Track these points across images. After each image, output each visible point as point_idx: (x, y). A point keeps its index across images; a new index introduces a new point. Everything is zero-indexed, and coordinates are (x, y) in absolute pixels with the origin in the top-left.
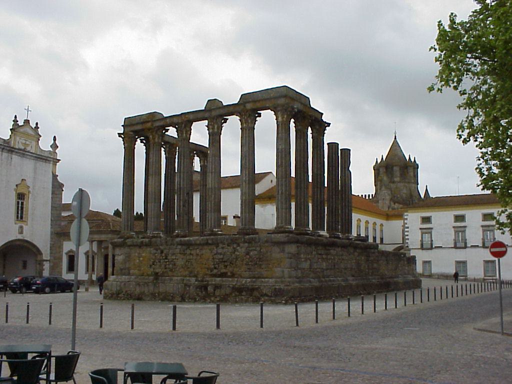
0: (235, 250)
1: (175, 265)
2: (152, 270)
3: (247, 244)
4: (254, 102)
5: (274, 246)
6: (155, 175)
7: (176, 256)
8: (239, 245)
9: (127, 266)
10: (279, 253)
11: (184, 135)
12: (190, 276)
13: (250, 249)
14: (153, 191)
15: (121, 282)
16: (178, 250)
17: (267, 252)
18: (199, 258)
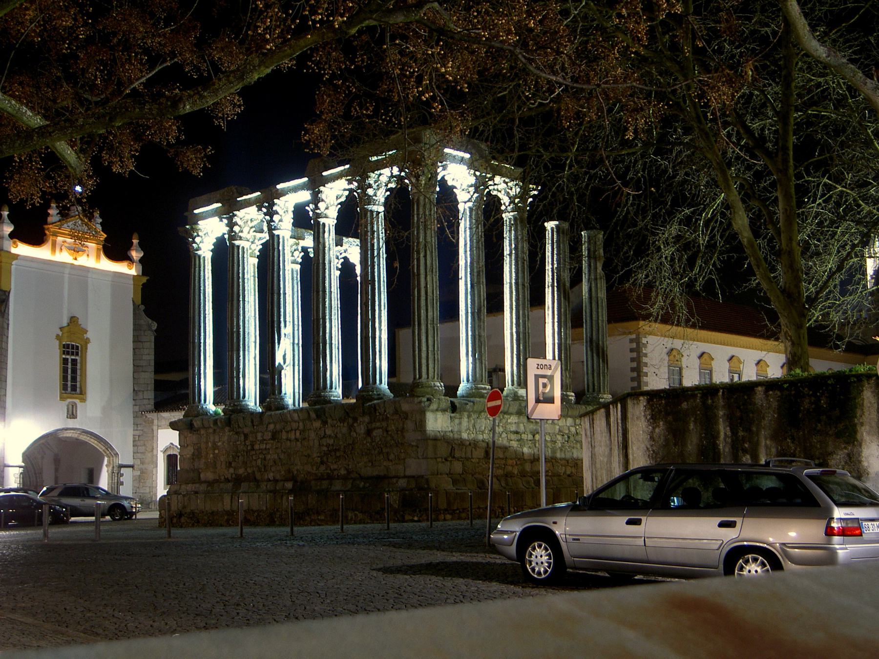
0: (351, 428)
1: (265, 459)
2: (232, 470)
3: (367, 419)
15: (184, 496)
16: (268, 435)
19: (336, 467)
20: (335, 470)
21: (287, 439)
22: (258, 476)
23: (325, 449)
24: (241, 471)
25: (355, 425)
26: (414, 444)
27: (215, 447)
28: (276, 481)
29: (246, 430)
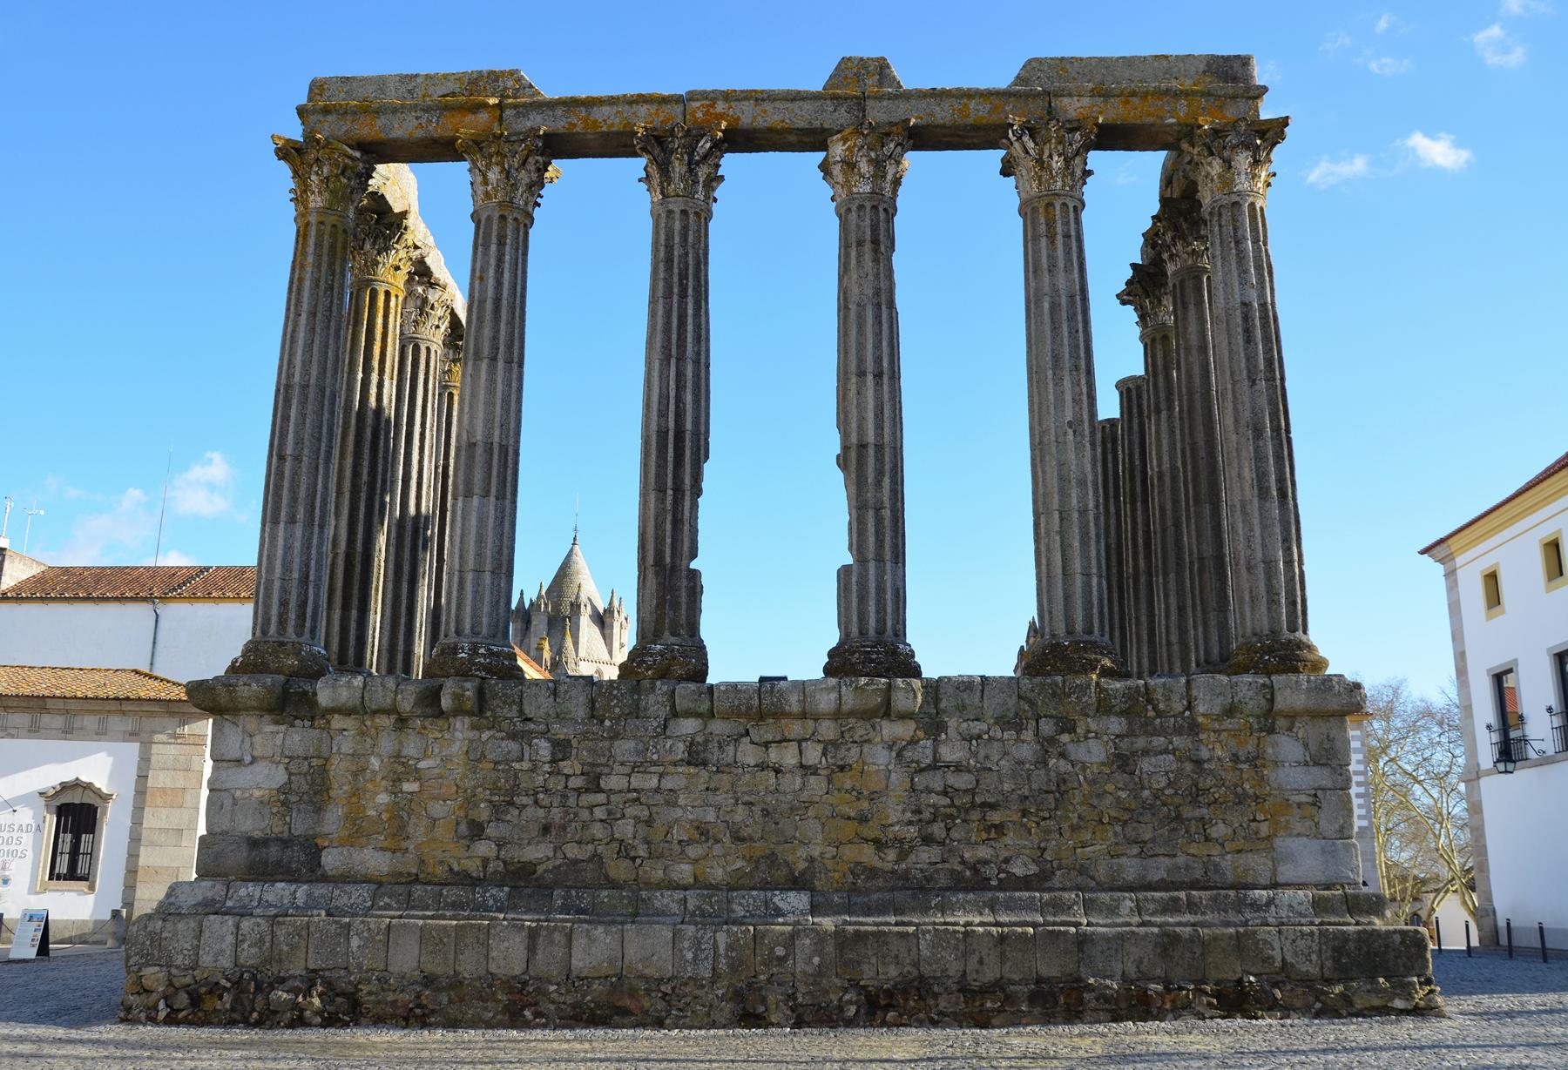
1: (649, 822)
2: (484, 848)
3: (1116, 725)
4: (1102, 93)
5: (1271, 731)
6: (509, 362)
7: (661, 776)
8: (1072, 729)
9: (299, 829)
10: (1306, 764)
11: (700, 195)
12: (766, 886)
13: (1141, 743)
14: (496, 439)
16: (680, 750)
17: (1235, 758)
18: (817, 784)
19: (984, 852)
20: (986, 862)
21: (762, 766)
22: (620, 870)
23: (933, 799)
24: (536, 852)
25: (1065, 738)
26: (1303, 798)
27: (401, 769)
28: (699, 883)
29: (561, 731)
